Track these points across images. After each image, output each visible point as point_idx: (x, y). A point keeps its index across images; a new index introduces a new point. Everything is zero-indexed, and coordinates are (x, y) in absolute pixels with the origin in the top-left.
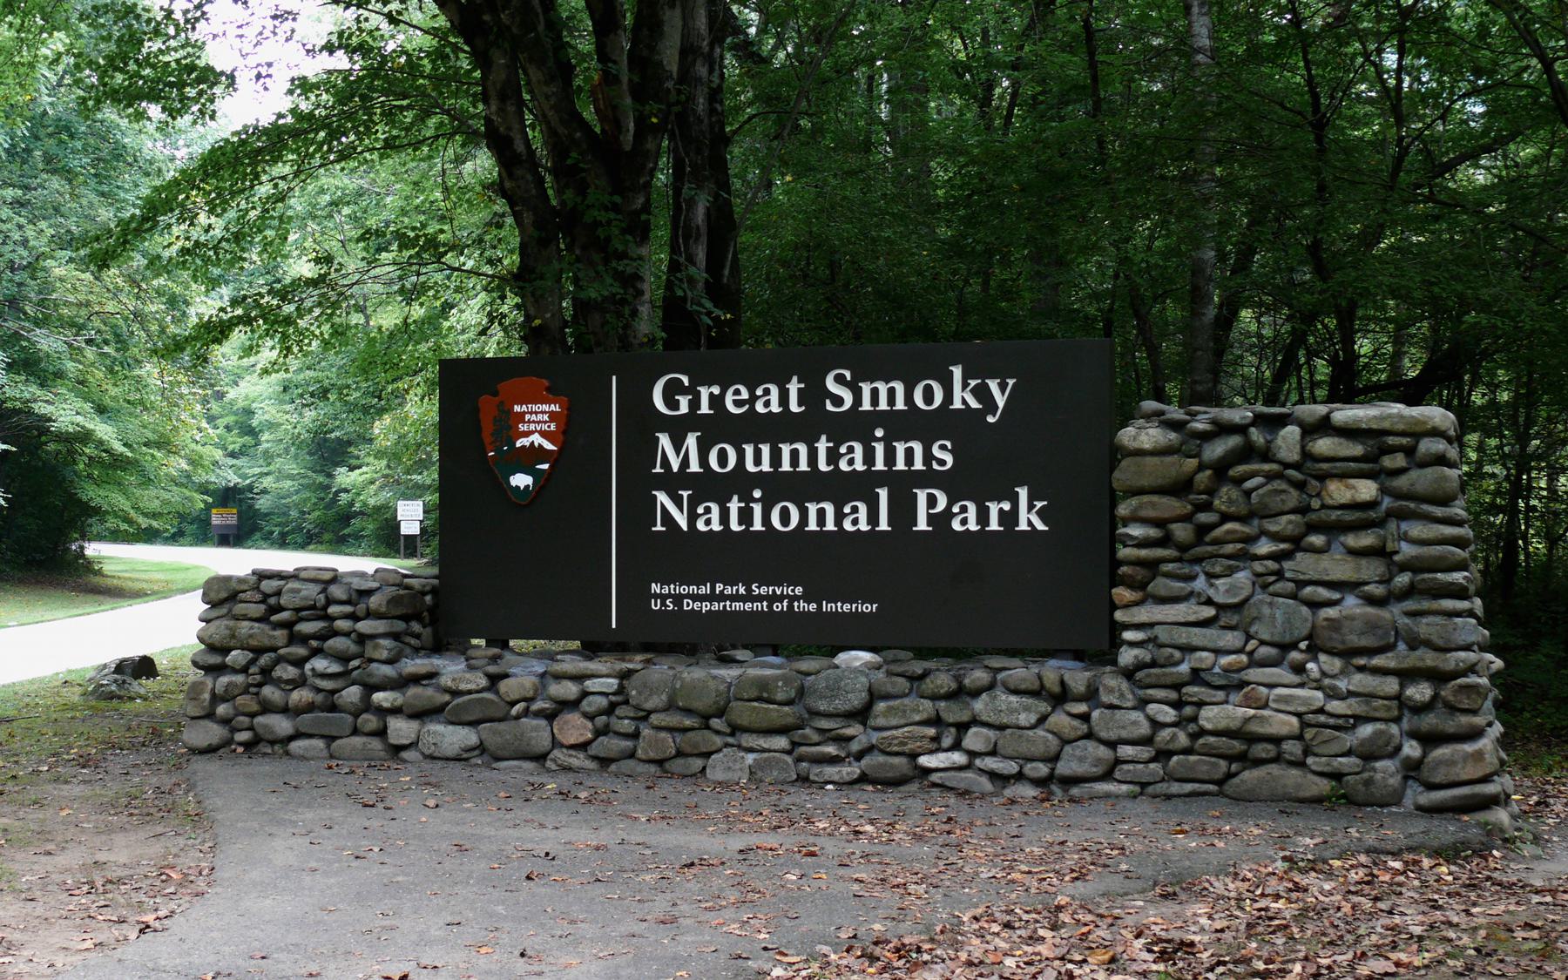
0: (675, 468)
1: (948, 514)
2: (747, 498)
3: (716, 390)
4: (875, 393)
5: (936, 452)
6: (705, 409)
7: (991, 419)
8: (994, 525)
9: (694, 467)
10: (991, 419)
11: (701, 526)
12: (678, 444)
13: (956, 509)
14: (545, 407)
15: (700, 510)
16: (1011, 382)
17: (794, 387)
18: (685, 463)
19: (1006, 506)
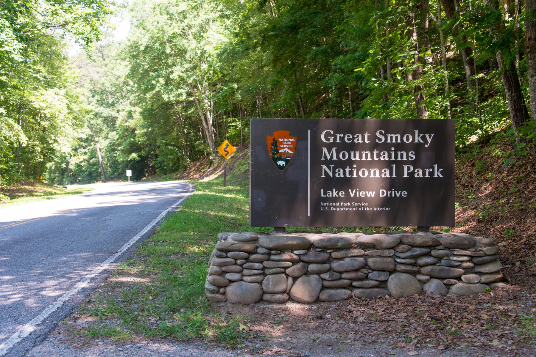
0: (329, 159)
1: (413, 172)
2: (351, 167)
3: (342, 135)
4: (391, 137)
5: (410, 155)
6: (338, 141)
7: (426, 146)
8: (427, 176)
9: (335, 158)
10: (426, 146)
11: (337, 176)
12: (329, 151)
13: (416, 171)
14: (290, 140)
15: (337, 171)
16: (432, 135)
17: (366, 135)
18: (332, 157)
19: (431, 170)
